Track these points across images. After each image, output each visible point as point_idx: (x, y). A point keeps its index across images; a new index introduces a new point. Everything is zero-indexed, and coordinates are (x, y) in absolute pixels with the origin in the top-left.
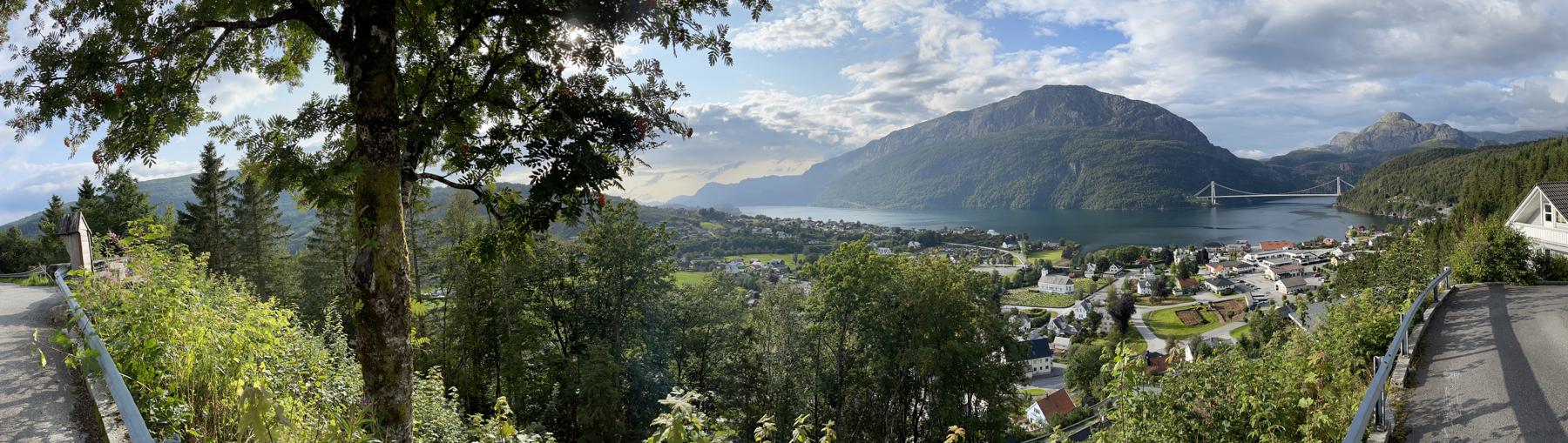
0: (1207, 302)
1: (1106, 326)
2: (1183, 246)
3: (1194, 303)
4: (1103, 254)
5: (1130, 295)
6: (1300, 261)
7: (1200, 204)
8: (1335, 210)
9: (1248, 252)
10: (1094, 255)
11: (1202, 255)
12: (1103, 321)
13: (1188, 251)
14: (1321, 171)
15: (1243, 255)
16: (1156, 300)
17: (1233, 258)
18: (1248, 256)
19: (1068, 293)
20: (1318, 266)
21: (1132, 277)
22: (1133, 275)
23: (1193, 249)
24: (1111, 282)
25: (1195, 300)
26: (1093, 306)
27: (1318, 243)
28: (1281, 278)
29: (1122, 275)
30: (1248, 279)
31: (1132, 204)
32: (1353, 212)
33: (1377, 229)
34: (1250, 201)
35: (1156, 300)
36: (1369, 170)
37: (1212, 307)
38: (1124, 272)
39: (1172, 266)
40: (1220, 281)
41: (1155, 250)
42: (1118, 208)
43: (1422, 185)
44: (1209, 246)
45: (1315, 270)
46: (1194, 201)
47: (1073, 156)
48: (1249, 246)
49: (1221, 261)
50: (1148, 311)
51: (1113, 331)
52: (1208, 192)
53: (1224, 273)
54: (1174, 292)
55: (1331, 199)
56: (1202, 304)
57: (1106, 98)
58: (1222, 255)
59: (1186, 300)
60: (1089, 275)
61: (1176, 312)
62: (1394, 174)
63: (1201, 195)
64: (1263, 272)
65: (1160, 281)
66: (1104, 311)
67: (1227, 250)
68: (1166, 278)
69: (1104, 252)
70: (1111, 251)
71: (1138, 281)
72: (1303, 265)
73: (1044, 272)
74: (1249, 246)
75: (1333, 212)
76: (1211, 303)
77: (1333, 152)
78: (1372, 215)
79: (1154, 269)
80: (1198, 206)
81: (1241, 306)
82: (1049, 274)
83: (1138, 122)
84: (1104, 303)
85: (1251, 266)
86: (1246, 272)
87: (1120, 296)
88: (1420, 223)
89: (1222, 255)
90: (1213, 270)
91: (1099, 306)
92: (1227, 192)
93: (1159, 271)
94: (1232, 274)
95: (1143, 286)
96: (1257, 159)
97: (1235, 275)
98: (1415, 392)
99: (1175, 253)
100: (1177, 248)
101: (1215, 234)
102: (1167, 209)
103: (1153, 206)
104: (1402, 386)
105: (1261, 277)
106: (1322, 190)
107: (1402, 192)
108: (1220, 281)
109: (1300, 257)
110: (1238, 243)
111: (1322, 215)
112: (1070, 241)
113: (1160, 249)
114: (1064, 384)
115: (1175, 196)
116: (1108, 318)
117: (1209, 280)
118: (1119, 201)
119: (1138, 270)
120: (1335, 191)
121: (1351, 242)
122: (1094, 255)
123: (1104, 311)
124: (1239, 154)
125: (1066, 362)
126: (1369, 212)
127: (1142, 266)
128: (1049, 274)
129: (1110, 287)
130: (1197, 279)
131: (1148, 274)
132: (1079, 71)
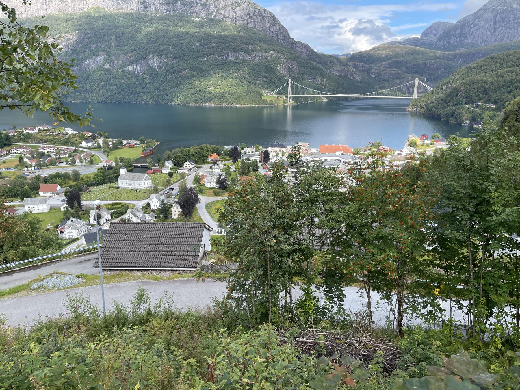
52: (284, 91)
63: (279, 93)
73: (123, 171)
92: (300, 92)
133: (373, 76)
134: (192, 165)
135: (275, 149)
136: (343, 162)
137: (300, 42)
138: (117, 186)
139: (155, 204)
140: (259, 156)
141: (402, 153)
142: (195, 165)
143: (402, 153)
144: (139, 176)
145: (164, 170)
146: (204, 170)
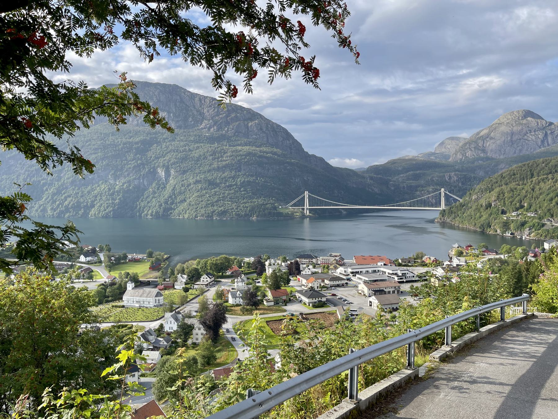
0: (298, 313)
1: (197, 336)
2: (276, 256)
3: (284, 314)
4: (194, 264)
5: (221, 304)
6: (396, 278)
7: (292, 214)
8: (437, 225)
9: (341, 265)
10: (185, 266)
11: (294, 266)
12: (194, 332)
13: (280, 262)
14: (422, 182)
15: (336, 268)
16: (247, 310)
17: (326, 270)
18: (341, 270)
19: (157, 306)
20: (415, 285)
21: (223, 287)
22: (224, 285)
23: (285, 260)
24: (203, 292)
25: (285, 311)
26: (184, 317)
27: (417, 260)
28: (375, 294)
29: (213, 285)
30: (341, 293)
31: (224, 213)
32: (458, 228)
33: (488, 250)
34: (344, 213)
35: (247, 310)
36: (481, 180)
37: (303, 318)
38: (216, 283)
39: (263, 276)
40: (312, 293)
41: (247, 260)
42: (210, 216)
43: (551, 199)
44: (302, 257)
45: (412, 287)
46: (287, 211)
47: (161, 160)
48: (343, 259)
49: (313, 273)
50: (238, 321)
51: (204, 341)
53: (316, 285)
54: (265, 303)
55: (433, 213)
56: (292, 315)
57: (197, 99)
58: (314, 267)
59: (277, 311)
60: (179, 286)
61: (267, 322)
62: (513, 185)
64: (356, 286)
65: (252, 290)
66: (195, 322)
67: (319, 262)
68: (257, 288)
69: (195, 262)
70: (203, 261)
71: (228, 291)
72: (399, 282)
74: (343, 259)
75: (436, 228)
76: (301, 314)
77: (437, 160)
78: (483, 233)
79: (245, 279)
80: (290, 217)
81: (332, 319)
82: (136, 287)
83: (231, 127)
84: (195, 314)
85: (343, 279)
86: (338, 286)
87: (211, 306)
88: (546, 246)
89: (314, 267)
90: (304, 281)
91: (190, 317)
93: (251, 281)
94: (324, 287)
95: (234, 296)
96: (354, 169)
97: (327, 288)
98: (448, 365)
99: (267, 263)
100: (269, 258)
101: (308, 245)
102: (259, 218)
103: (246, 215)
104: (438, 360)
105: (354, 291)
106: (425, 203)
107: (522, 207)
108: (312, 293)
109: (396, 274)
110: (331, 256)
111: (423, 231)
112: (158, 253)
113: (252, 259)
114: (153, 397)
115: (268, 206)
116: (199, 329)
117: (300, 292)
118: (210, 209)
119: (230, 280)
120: (438, 204)
121: (455, 262)
122: (185, 266)
123: (195, 322)
124: (334, 162)
125: (155, 375)
126: (478, 230)
127: (233, 276)
128: (136, 287)
129: (201, 297)
130: (289, 290)
131: (240, 284)
132: (167, 68)
133: (392, 188)
134: (210, 278)
135: (304, 261)
136: (389, 273)
137: (314, 156)
138: (121, 304)
139: (171, 326)
140: (288, 267)
141: (452, 263)
142: (213, 279)
143: (452, 263)
144: (150, 292)
145: (177, 285)
146: (226, 285)
